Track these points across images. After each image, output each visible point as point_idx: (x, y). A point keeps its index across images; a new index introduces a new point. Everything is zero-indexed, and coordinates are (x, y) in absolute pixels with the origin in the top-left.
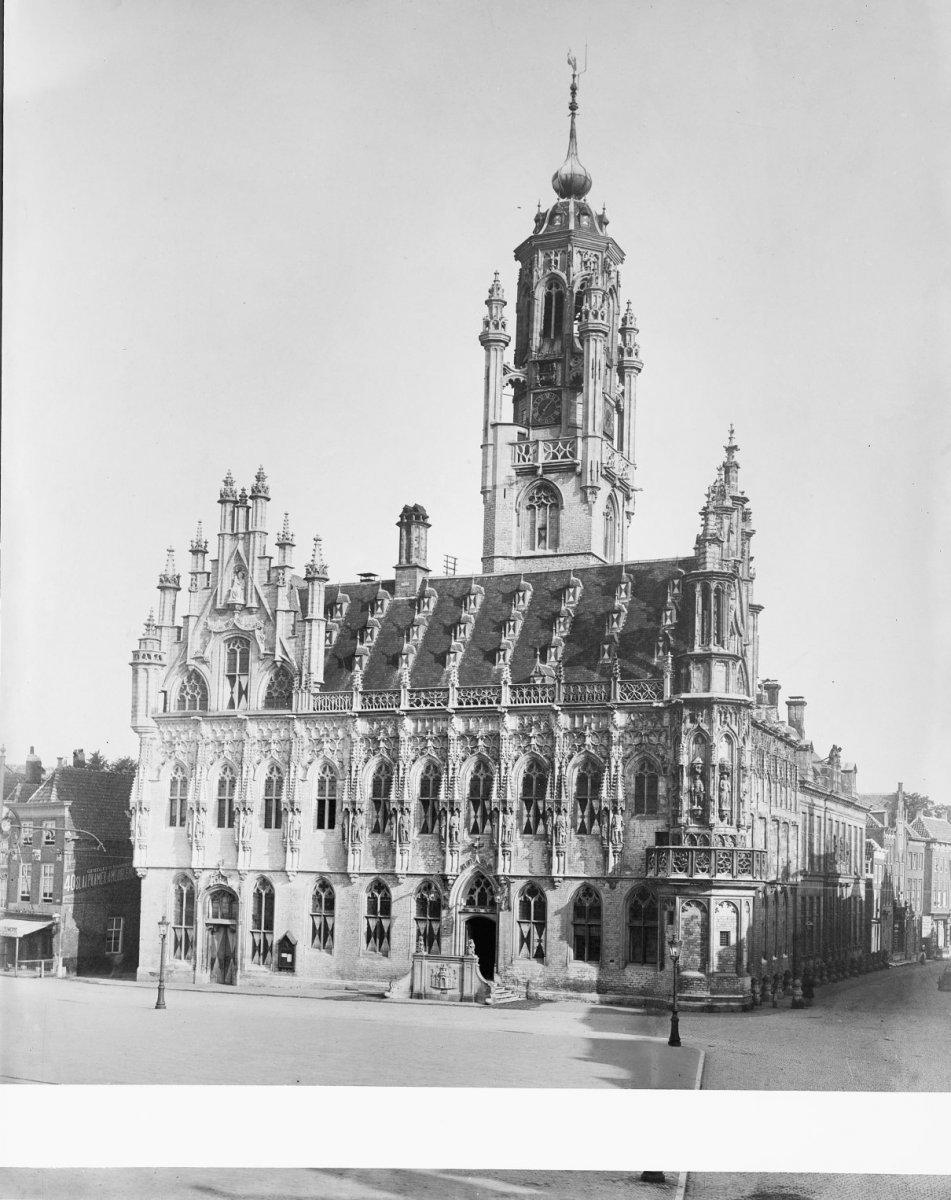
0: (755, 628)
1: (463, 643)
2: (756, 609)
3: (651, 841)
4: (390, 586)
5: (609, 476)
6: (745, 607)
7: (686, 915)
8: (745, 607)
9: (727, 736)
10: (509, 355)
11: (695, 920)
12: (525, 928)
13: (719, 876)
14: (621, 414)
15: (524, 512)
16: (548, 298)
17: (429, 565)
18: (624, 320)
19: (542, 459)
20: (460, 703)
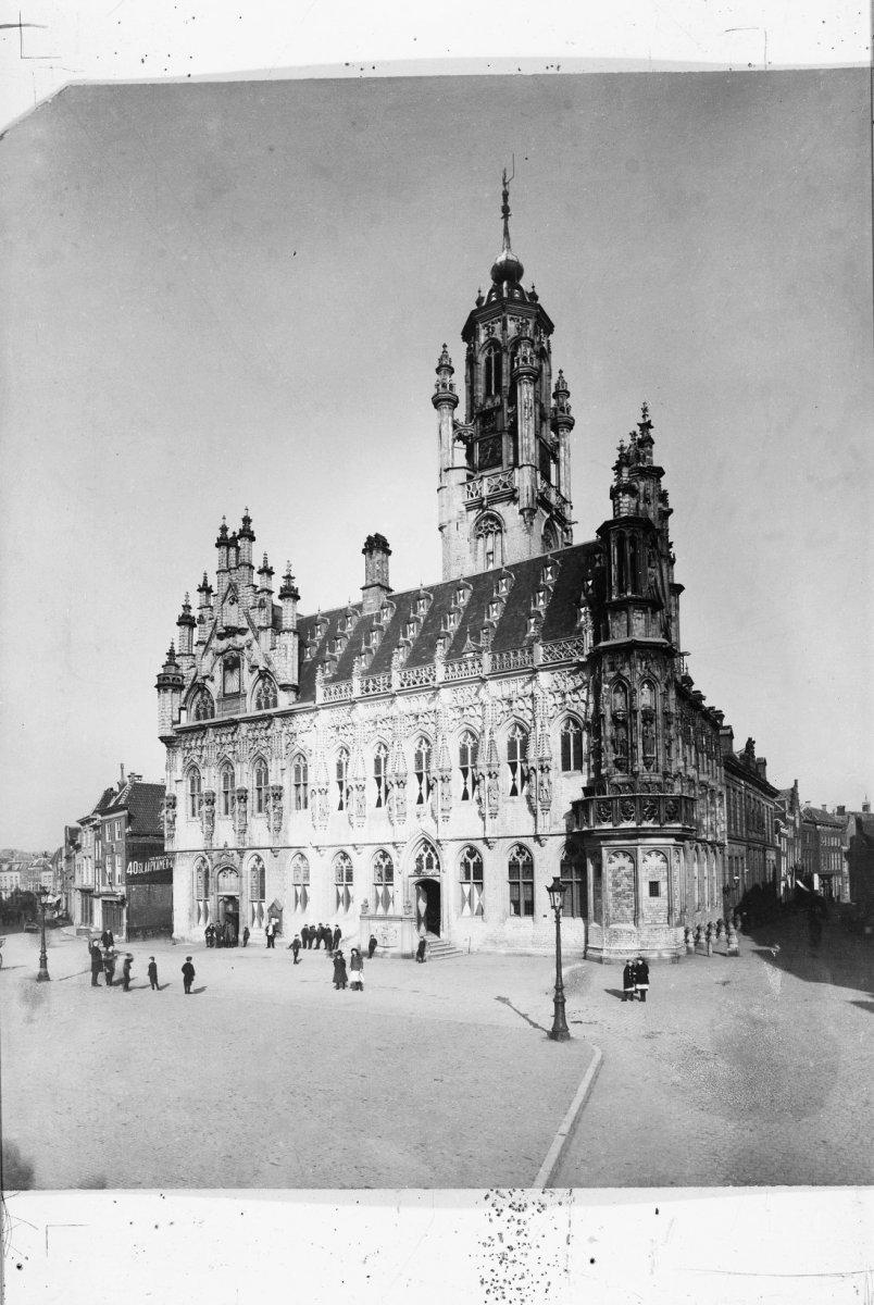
0: (677, 607)
1: (412, 639)
2: (678, 589)
3: (579, 795)
4: (359, 607)
5: (543, 502)
6: (666, 586)
7: (613, 866)
8: (666, 586)
9: (648, 682)
10: (461, 413)
11: (623, 871)
12: (467, 888)
13: (646, 824)
14: (557, 462)
15: (473, 540)
16: (488, 361)
17: (391, 586)
18: (557, 385)
19: (485, 492)
20: (402, 685)
